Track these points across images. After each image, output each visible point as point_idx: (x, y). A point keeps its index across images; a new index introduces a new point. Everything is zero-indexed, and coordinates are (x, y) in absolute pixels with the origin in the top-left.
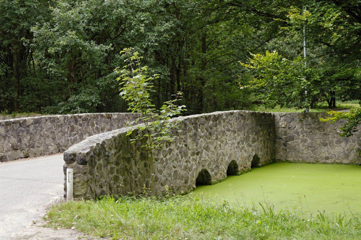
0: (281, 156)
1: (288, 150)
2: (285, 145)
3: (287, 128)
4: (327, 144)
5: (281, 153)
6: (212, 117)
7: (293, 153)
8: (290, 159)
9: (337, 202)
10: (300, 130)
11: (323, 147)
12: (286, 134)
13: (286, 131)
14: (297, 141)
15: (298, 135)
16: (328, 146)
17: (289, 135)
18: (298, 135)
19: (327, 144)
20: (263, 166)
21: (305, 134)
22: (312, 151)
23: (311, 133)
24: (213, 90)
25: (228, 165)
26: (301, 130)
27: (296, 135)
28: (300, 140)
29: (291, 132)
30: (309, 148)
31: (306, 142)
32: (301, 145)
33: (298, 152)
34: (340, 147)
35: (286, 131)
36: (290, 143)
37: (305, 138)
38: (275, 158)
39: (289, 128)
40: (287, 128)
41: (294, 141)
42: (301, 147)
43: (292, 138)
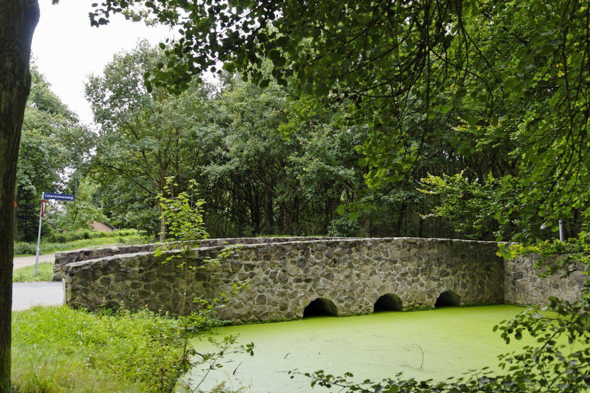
0: (509, 296)
1: (517, 290)
2: (514, 283)
3: (516, 262)
4: (558, 285)
5: (510, 293)
6: (74, 260)
7: (522, 294)
8: (518, 302)
9: (466, 373)
10: (529, 266)
11: (553, 290)
12: (514, 268)
13: (515, 266)
14: (526, 279)
15: (527, 272)
16: (560, 288)
17: (518, 271)
18: (527, 272)
19: (558, 285)
20: (464, 306)
21: (534, 271)
22: (543, 293)
23: (540, 270)
24: (170, 228)
25: (12, 314)
26: (530, 264)
27: (525, 271)
28: (529, 278)
29: (520, 267)
30: (539, 289)
31: (535, 281)
32: (530, 284)
33: (528, 293)
34: (573, 292)
35: (515, 266)
36: (518, 280)
37: (535, 276)
38: (503, 299)
39: (518, 262)
40: (516, 262)
41: (523, 278)
42: (530, 287)
43: (520, 276)
